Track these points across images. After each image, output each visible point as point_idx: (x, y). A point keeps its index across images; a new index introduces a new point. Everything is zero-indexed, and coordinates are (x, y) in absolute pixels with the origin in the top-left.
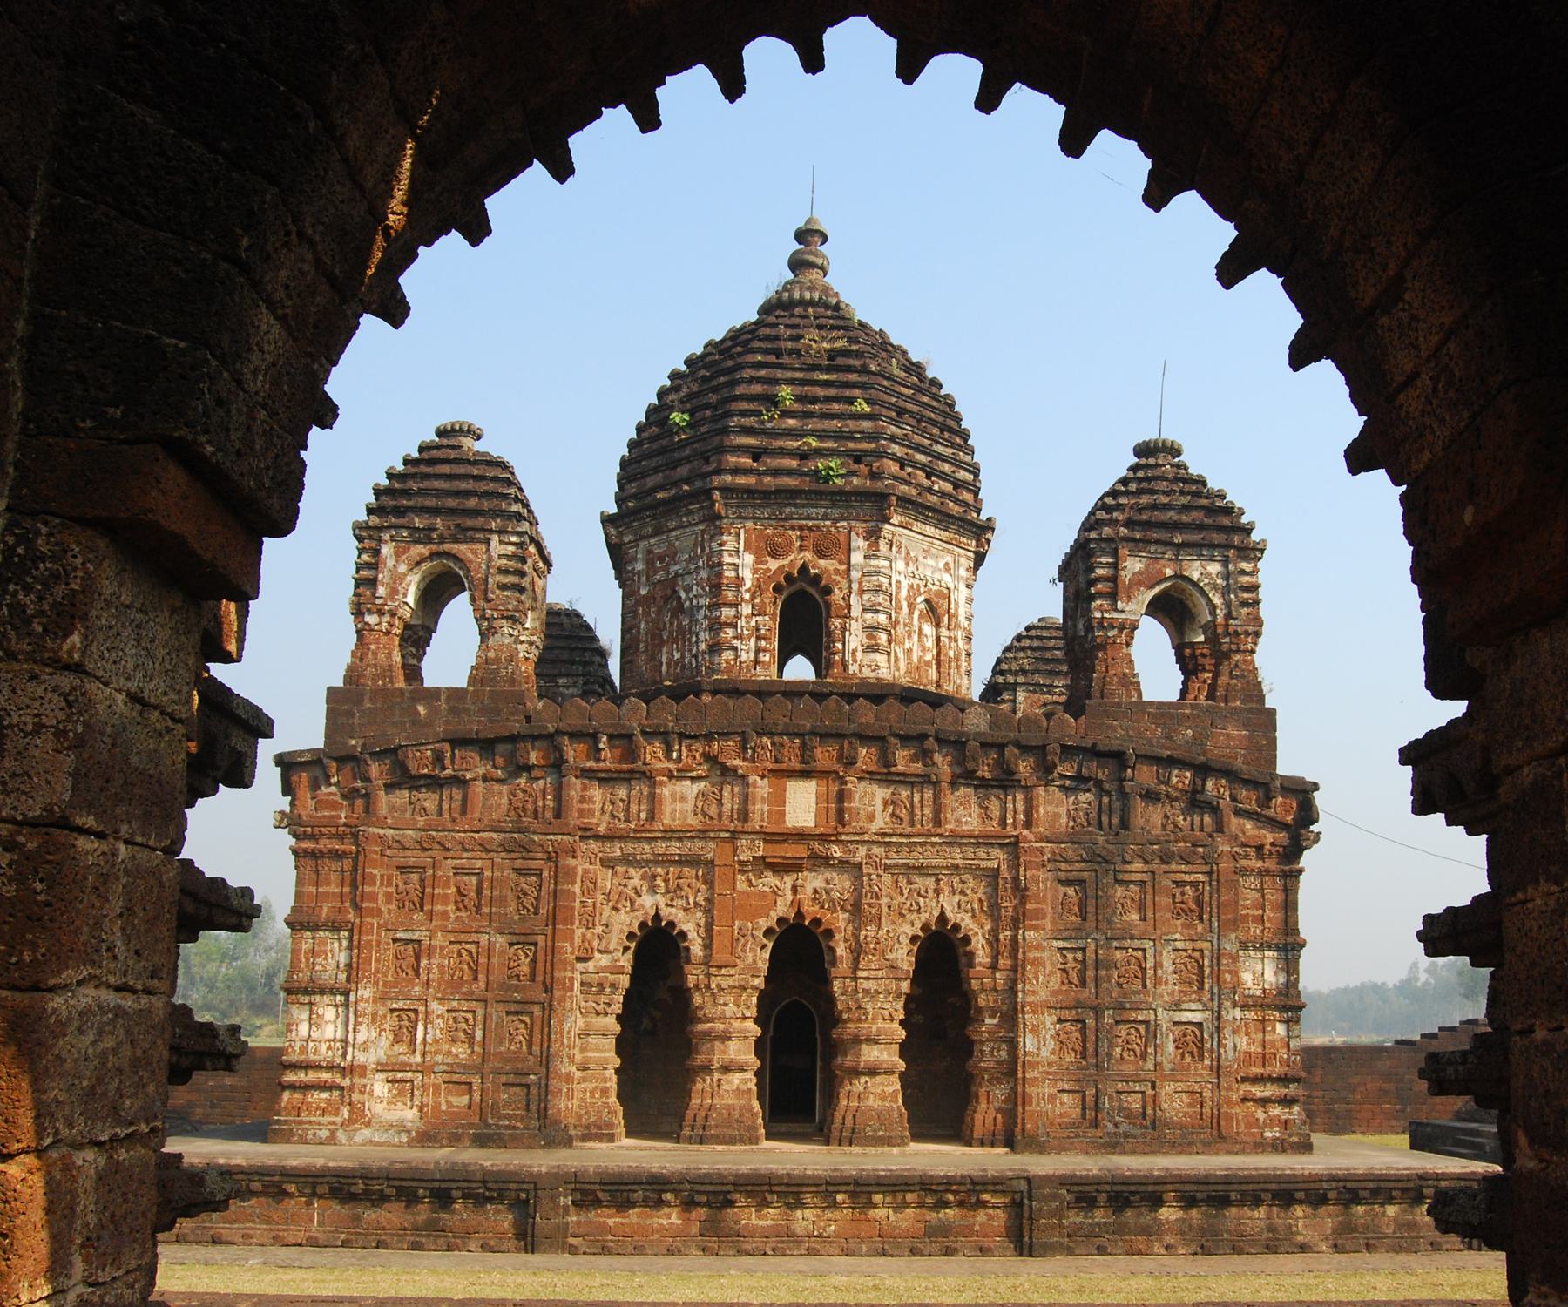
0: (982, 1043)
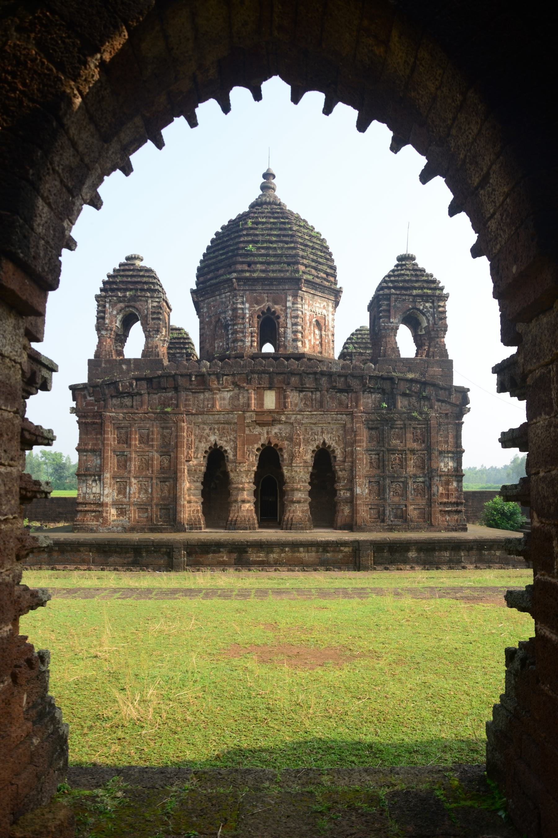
0: (340, 490)
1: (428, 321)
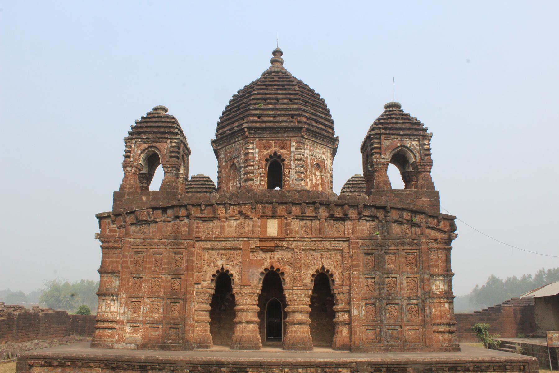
0: (338, 312)
1: (415, 156)
